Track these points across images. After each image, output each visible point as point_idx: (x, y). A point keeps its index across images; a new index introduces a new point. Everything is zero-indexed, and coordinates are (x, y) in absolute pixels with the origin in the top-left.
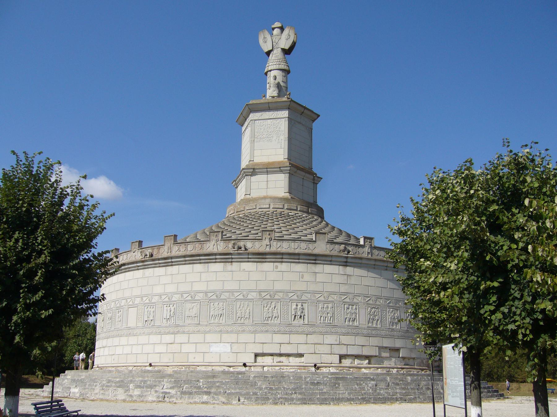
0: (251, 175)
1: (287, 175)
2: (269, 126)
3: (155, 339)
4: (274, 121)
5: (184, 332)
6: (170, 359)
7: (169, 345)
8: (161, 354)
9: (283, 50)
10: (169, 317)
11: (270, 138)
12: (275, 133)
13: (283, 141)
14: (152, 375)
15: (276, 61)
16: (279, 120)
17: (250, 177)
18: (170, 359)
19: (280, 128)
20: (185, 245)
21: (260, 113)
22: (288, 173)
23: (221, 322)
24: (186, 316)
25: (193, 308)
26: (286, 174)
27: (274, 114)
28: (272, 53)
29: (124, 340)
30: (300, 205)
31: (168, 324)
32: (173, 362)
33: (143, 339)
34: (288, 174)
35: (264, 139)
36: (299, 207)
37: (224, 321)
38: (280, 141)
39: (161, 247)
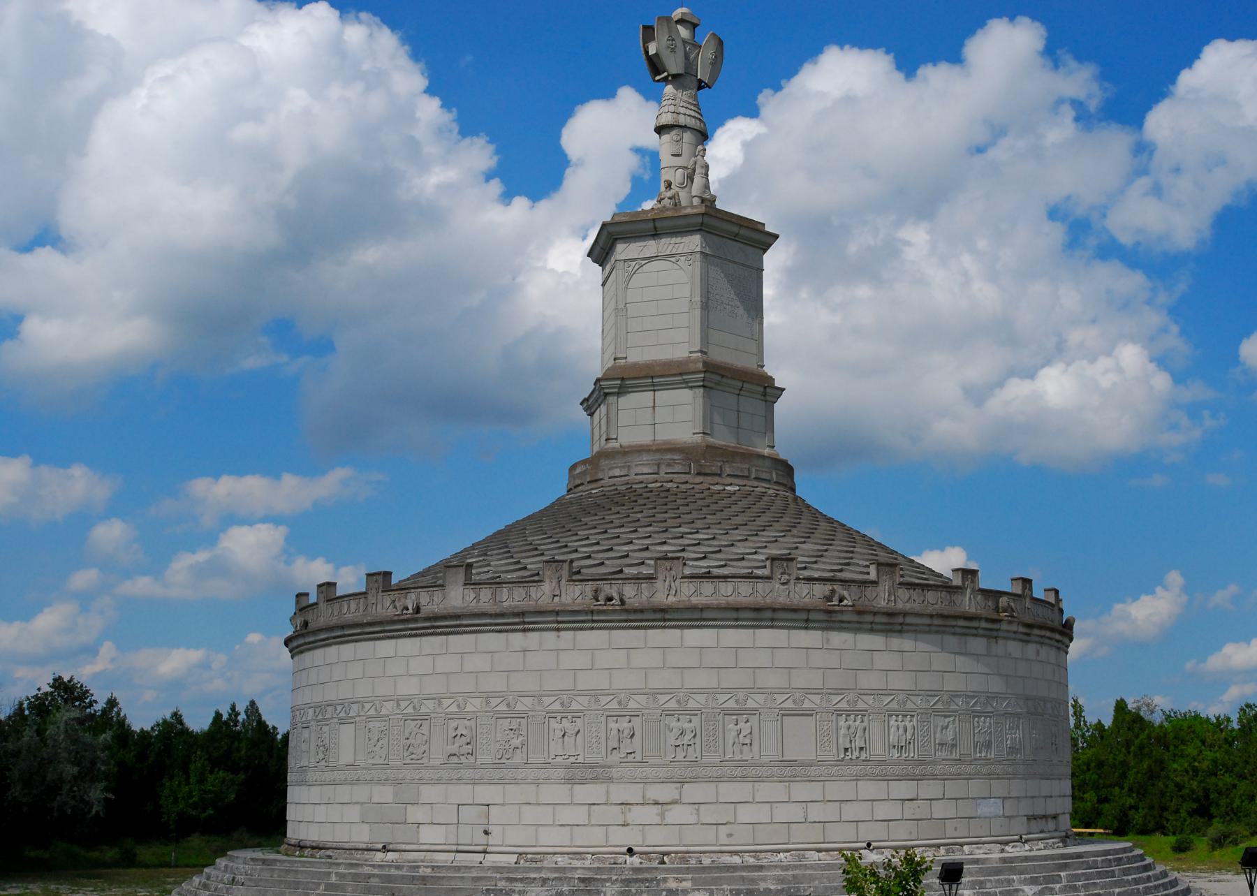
3: (869, 789)
5: (934, 777)
6: (911, 833)
7: (907, 802)
8: (890, 823)
10: (904, 744)
14: (978, 869)
18: (911, 833)
20: (923, 590)
23: (989, 757)
24: (937, 742)
25: (947, 727)
29: (767, 791)
31: (903, 758)
32: (917, 840)
33: (837, 790)
37: (993, 756)
39: (869, 585)
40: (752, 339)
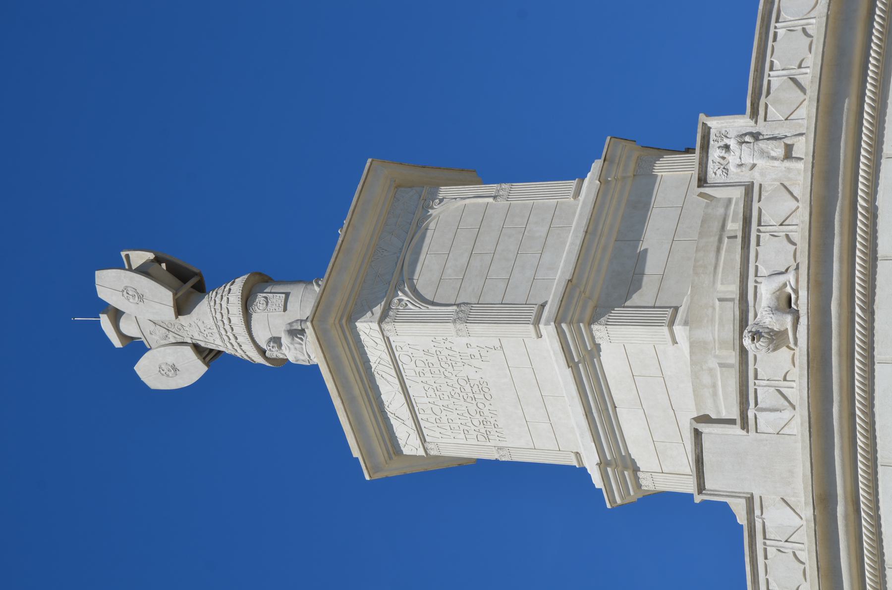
0: (636, 470)
1: (599, 331)
2: (430, 392)
4: (409, 373)
9: (181, 308)
11: (475, 389)
12: (450, 369)
13: (473, 341)
15: (223, 332)
16: (403, 358)
17: (640, 474)
19: (426, 352)
21: (393, 421)
22: (591, 331)
26: (597, 334)
27: (384, 375)
28: (203, 344)
30: (714, 282)
34: (595, 327)
35: (486, 413)
36: (719, 287)
38: (475, 351)
40: (501, 347)
